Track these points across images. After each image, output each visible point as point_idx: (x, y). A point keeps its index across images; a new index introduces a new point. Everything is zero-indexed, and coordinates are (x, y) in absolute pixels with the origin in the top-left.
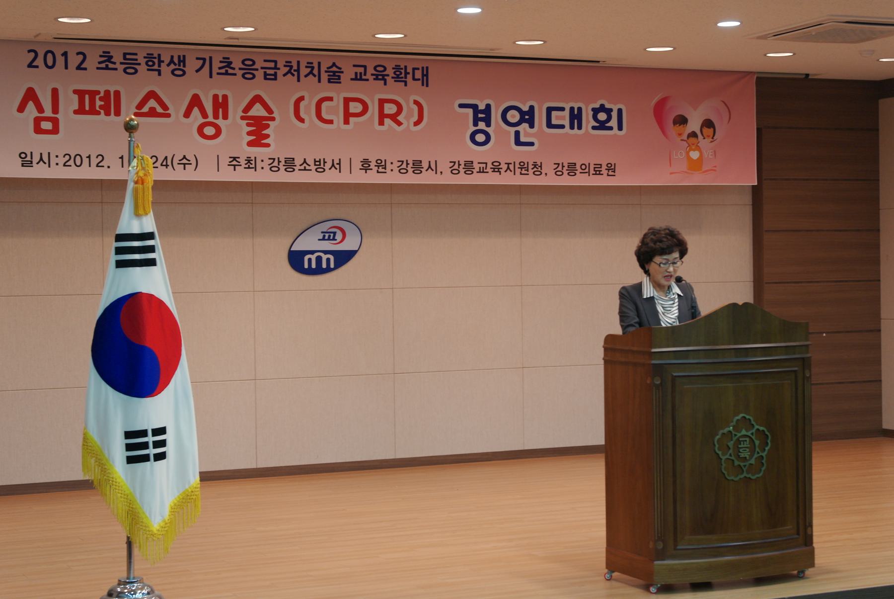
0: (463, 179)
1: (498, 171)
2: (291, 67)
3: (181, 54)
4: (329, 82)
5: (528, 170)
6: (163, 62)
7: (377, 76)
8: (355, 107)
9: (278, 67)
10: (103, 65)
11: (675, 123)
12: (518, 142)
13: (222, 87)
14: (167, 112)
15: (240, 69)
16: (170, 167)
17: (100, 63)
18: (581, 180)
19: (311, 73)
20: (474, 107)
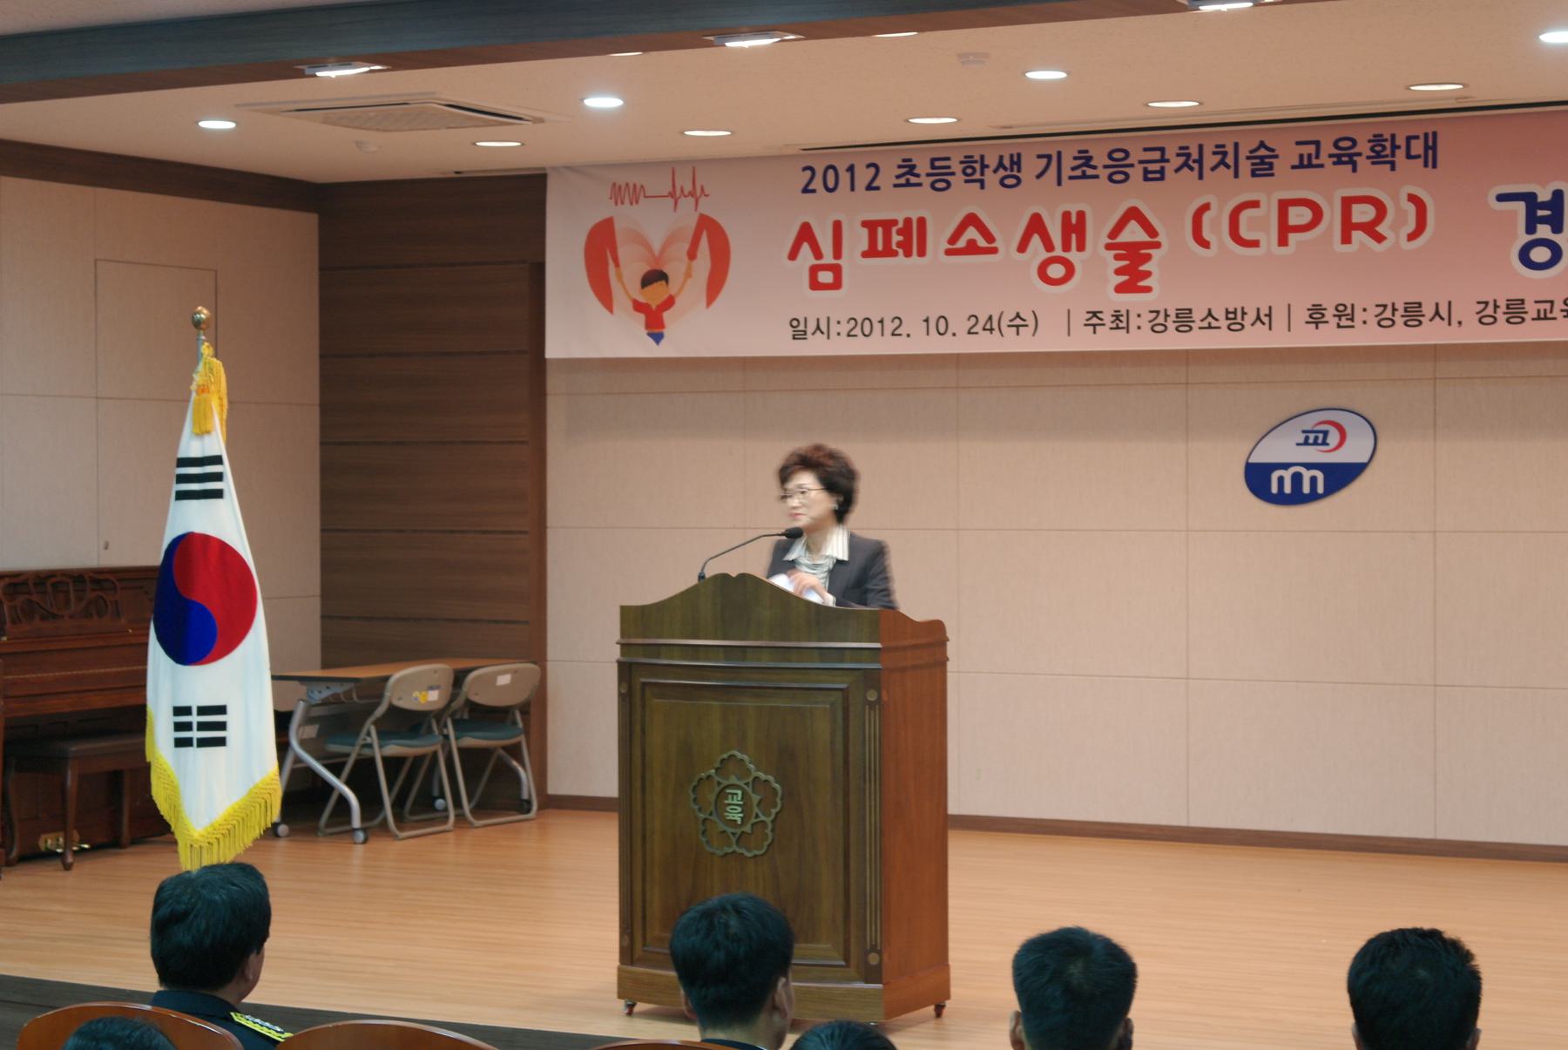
2: (1188, 156)
3: (1015, 152)
4: (1254, 174)
6: (987, 166)
8: (1299, 216)
9: (1166, 157)
10: (902, 181)
14: (954, 247)
15: (1106, 167)
16: (996, 332)
17: (898, 177)
19: (1222, 162)
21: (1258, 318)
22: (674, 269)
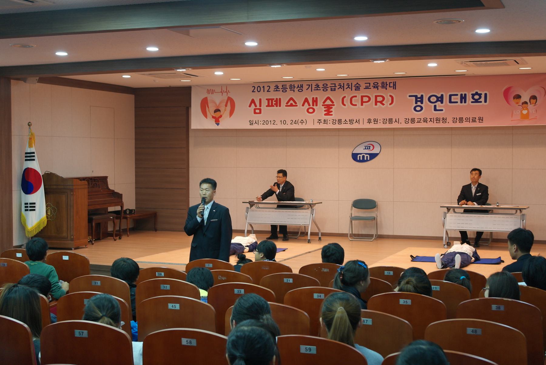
0: (410, 125)
1: (426, 122)
4: (355, 90)
5: (440, 121)
6: (295, 87)
7: (374, 86)
8: (366, 99)
9: (336, 86)
10: (276, 90)
11: (514, 98)
12: (435, 109)
13: (315, 94)
15: (322, 88)
17: (274, 89)
18: (465, 125)
19: (348, 87)
20: (416, 97)
21: (356, 121)
22: (222, 109)
